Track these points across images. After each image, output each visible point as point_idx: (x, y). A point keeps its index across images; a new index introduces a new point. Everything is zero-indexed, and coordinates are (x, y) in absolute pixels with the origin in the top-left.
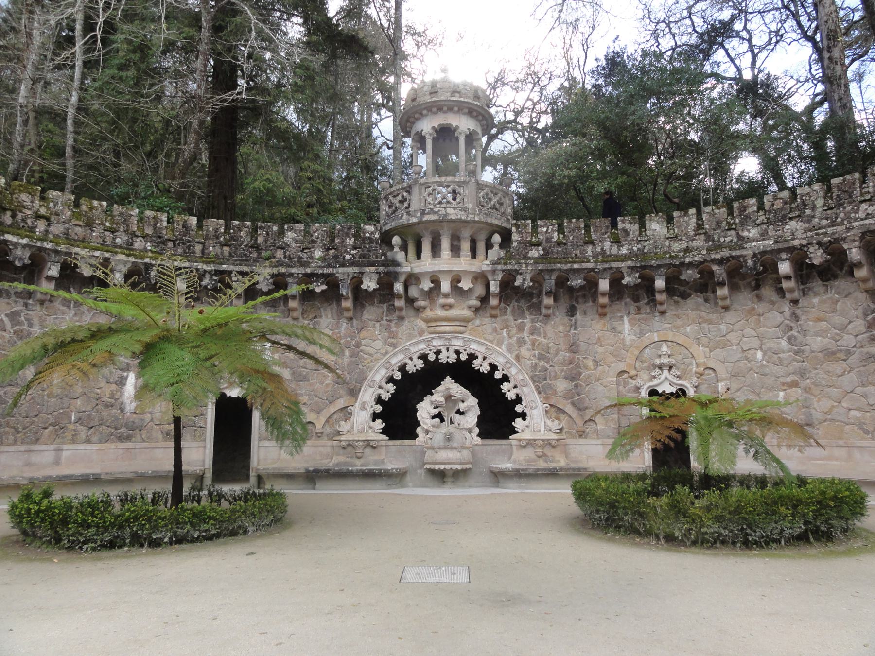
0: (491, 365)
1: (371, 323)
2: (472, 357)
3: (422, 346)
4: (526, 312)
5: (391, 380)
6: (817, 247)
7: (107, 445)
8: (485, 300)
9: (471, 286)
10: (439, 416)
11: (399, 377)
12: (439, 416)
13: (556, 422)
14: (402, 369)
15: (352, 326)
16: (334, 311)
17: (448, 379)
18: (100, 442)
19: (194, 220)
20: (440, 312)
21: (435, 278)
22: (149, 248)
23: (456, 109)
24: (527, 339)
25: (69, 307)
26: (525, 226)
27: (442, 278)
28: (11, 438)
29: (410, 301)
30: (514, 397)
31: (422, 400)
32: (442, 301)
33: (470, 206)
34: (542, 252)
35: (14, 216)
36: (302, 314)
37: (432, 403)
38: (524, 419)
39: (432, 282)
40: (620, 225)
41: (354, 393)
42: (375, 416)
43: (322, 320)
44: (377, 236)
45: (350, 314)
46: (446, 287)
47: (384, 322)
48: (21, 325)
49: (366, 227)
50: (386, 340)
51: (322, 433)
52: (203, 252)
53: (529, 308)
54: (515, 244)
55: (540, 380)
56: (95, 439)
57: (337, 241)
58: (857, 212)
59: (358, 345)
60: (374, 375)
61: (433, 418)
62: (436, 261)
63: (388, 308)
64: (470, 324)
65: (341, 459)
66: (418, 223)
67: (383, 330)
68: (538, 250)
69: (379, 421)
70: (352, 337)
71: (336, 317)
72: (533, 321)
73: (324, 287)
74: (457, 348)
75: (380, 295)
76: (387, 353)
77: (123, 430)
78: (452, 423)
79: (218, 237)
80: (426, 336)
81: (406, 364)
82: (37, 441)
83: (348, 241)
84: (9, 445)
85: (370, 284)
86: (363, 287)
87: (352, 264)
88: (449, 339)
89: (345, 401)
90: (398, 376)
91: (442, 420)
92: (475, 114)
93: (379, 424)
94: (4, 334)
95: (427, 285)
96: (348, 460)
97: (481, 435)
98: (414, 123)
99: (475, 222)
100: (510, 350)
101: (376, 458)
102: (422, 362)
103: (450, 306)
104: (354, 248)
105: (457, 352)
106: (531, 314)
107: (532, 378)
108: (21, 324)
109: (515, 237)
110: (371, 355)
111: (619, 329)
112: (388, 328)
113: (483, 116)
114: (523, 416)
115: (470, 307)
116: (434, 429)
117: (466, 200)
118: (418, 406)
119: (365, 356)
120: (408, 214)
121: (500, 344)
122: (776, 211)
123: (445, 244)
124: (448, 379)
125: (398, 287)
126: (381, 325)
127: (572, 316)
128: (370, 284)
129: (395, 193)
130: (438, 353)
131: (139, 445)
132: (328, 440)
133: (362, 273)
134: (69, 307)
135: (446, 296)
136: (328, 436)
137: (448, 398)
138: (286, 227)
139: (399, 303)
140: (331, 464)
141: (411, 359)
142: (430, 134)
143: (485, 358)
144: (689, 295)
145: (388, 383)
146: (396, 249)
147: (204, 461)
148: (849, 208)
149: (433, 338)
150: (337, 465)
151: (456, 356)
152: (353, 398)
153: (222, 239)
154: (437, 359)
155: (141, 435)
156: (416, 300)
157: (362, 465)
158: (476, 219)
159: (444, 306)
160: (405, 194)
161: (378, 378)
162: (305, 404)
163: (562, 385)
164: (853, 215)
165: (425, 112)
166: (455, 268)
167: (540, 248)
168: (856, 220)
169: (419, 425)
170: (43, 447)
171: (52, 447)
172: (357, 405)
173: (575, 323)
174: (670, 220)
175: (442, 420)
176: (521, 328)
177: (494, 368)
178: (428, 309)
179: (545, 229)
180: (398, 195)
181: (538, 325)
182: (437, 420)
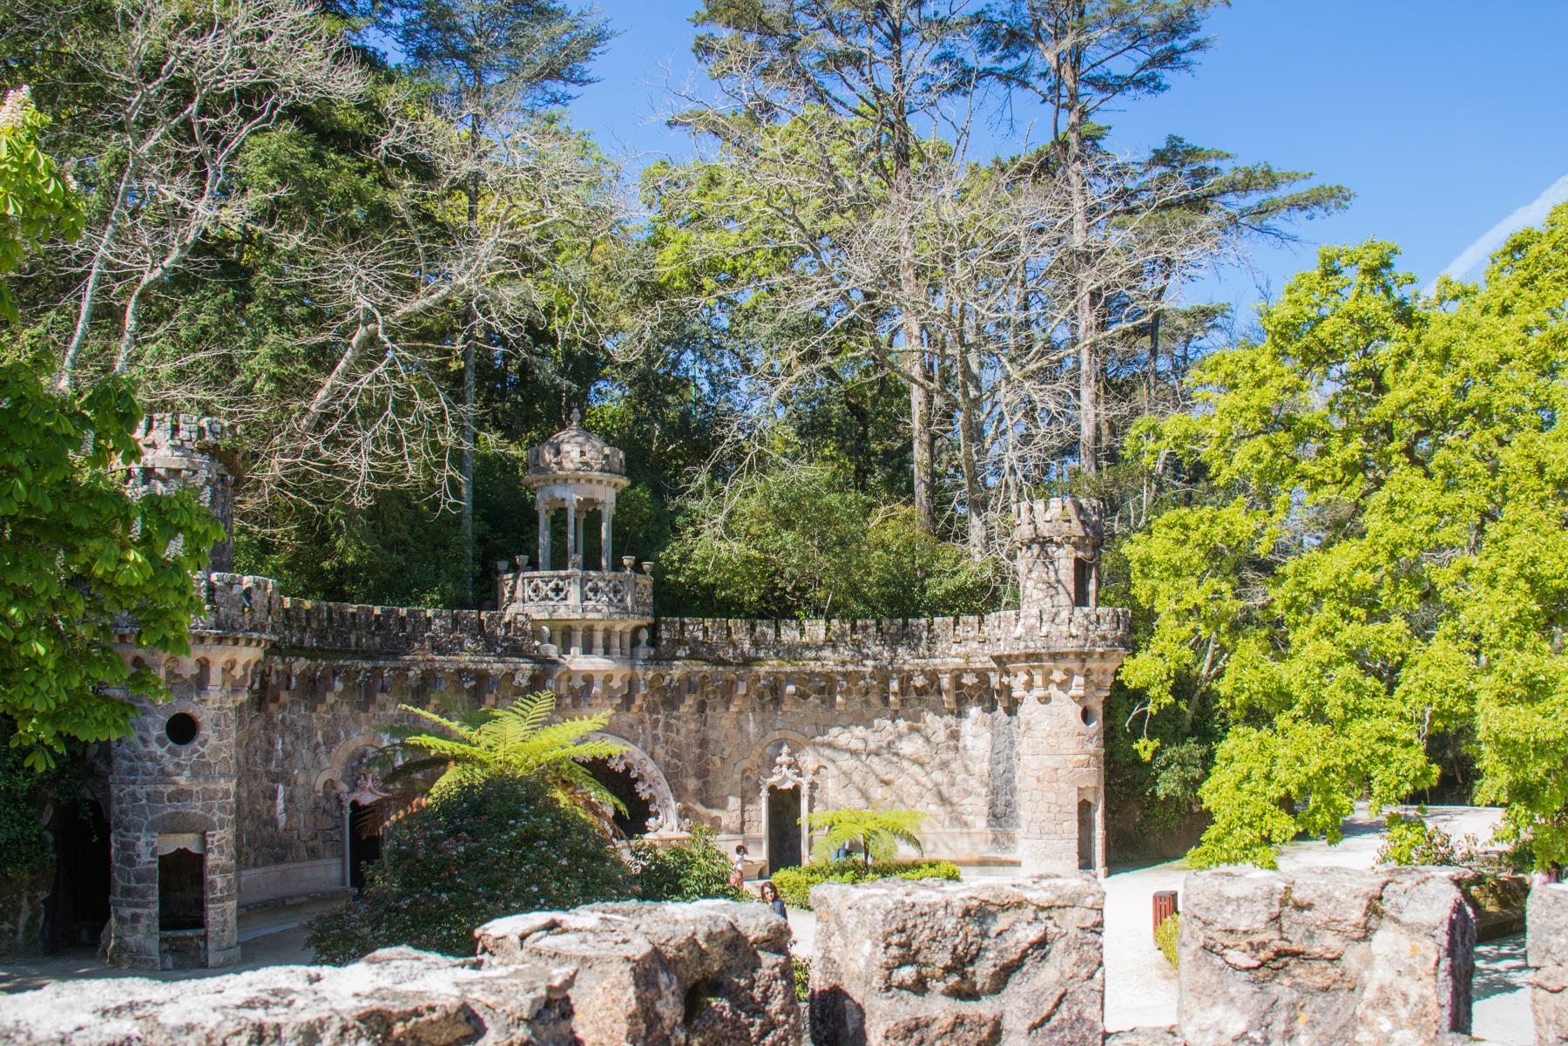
8: (628, 700)
26: (673, 623)
53: (663, 703)
55: (674, 778)
77: (277, 849)
79: (369, 626)
100: (644, 748)
109: (665, 635)
121: (635, 742)
123: (599, 639)
163: (692, 784)
176: (655, 723)
181: (672, 721)
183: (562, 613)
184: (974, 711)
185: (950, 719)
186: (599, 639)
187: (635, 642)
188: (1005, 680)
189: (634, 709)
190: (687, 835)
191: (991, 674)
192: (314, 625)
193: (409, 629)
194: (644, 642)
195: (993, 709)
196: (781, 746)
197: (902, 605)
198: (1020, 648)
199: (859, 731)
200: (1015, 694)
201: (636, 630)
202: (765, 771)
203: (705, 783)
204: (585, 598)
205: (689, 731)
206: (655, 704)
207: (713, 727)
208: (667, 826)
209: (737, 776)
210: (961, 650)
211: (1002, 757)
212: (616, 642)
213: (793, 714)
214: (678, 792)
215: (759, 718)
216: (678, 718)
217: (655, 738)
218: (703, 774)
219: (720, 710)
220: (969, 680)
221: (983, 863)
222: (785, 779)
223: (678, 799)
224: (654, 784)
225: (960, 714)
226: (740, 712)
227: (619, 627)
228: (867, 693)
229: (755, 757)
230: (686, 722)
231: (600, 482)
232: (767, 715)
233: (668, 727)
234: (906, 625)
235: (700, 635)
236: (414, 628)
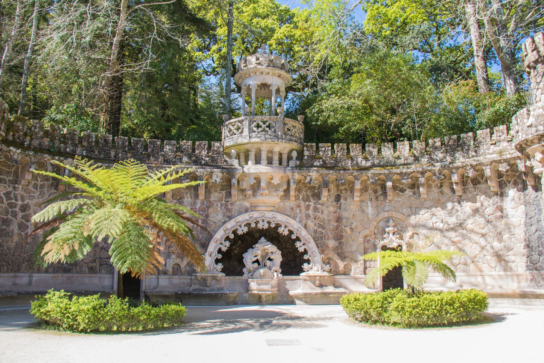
0: (289, 230)
2: (278, 226)
4: (311, 198)
5: (227, 238)
6: (470, 167)
8: (287, 191)
10: (257, 261)
13: (328, 266)
14: (234, 232)
15: (203, 204)
16: (192, 195)
22: (85, 154)
24: (311, 214)
25: (37, 189)
28: (6, 268)
30: (303, 251)
31: (247, 252)
33: (280, 133)
34: (321, 163)
36: (172, 196)
38: (309, 264)
40: (367, 149)
42: (217, 261)
50: (224, 214)
52: (115, 156)
54: (306, 157)
55: (319, 240)
57: (197, 152)
58: (489, 149)
59: (207, 216)
61: (254, 262)
62: (258, 166)
65: (197, 287)
67: (223, 208)
68: (319, 161)
69: (221, 264)
72: (315, 203)
74: (268, 220)
76: (225, 223)
78: (265, 266)
79: (124, 148)
82: (19, 271)
84: (5, 272)
90: (232, 236)
93: (220, 266)
96: (202, 287)
97: (284, 273)
100: (301, 222)
101: (218, 286)
105: (269, 223)
106: (314, 200)
107: (314, 239)
108: (12, 199)
109: (306, 153)
111: (365, 210)
114: (308, 261)
117: (277, 130)
118: (243, 255)
121: (294, 218)
122: (450, 145)
125: (234, 181)
127: (338, 201)
129: (233, 124)
130: (257, 223)
131: (75, 275)
134: (37, 189)
138: (165, 142)
140: (191, 290)
141: (240, 226)
143: (286, 227)
144: (405, 190)
147: (113, 286)
148: (485, 147)
150: (195, 290)
152: (204, 250)
153: (127, 149)
155: (76, 269)
157: (209, 291)
160: (240, 124)
163: (332, 243)
164: (487, 151)
165: (252, 74)
167: (321, 160)
168: (489, 154)
169: (245, 267)
170: (22, 274)
171: (27, 274)
172: (207, 254)
173: (340, 206)
174: (395, 147)
176: (308, 207)
177: (291, 232)
179: (323, 149)
182: (256, 264)
183: (240, 140)
184: (512, 192)
185: (496, 199)
186: (264, 156)
187: (290, 158)
188: (528, 163)
189: (292, 198)
190: (326, 274)
191: (518, 161)
192: (85, 144)
193: (149, 150)
194: (294, 158)
195: (525, 188)
196: (388, 221)
197: (460, 128)
198: (531, 134)
199: (439, 212)
200: (536, 171)
201: (291, 151)
202: (379, 236)
203: (340, 243)
204: (251, 131)
205: (329, 212)
206: (307, 195)
207: (345, 210)
208: (315, 268)
209: (361, 240)
210: (497, 149)
211: (534, 220)
212: (276, 158)
213: (396, 202)
214: (322, 248)
215: (374, 204)
216: (323, 205)
217: (308, 216)
218: (339, 237)
219: (349, 200)
220: (503, 168)
221: (524, 296)
222: (392, 241)
223: (322, 252)
224: (306, 243)
225: (502, 195)
226: (362, 201)
227: (277, 149)
228: (441, 186)
229: (372, 228)
230: (327, 207)
231: (268, 73)
232: (379, 202)
233: (316, 209)
234: (459, 138)
235: (330, 152)
236: (153, 150)
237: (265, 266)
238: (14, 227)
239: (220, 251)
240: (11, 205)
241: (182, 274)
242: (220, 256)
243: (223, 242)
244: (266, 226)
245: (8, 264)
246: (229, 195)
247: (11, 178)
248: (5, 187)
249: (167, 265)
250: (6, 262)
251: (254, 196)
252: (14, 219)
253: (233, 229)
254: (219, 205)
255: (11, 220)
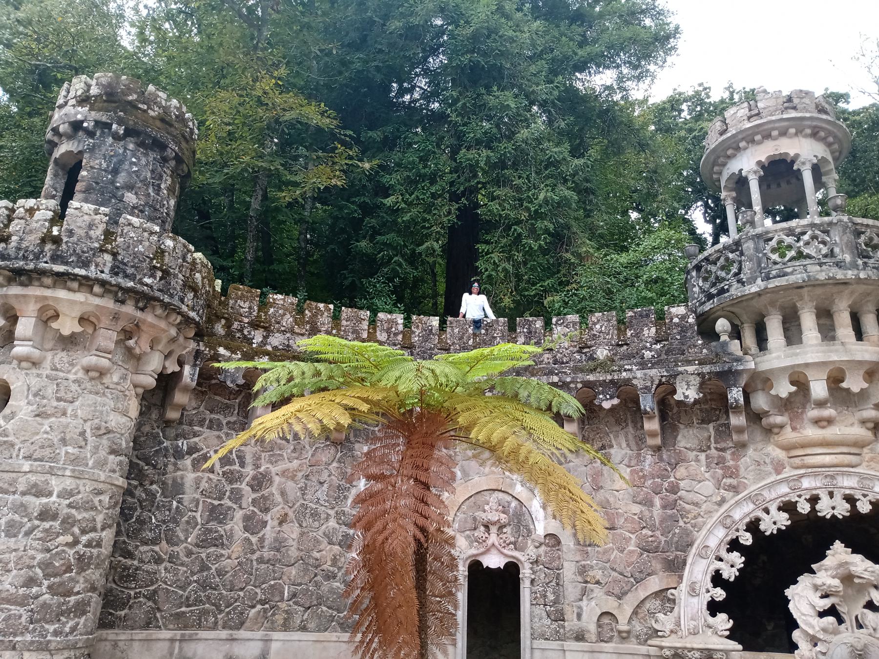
1: (692, 455)
3: (784, 489)
5: (734, 545)
7: (326, 635)
9: (865, 385)
10: (832, 611)
11: (749, 542)
12: (832, 611)
14: (753, 527)
15: (661, 459)
16: (630, 437)
17: (838, 545)
18: (319, 631)
19: (435, 321)
20: (811, 433)
21: (796, 378)
23: (792, 131)
27: (811, 375)
29: (756, 417)
32: (813, 413)
35: (228, 326)
37: (816, 588)
39: (793, 383)
41: (676, 567)
43: (612, 451)
44: (691, 320)
45: (658, 441)
46: (819, 389)
47: (713, 452)
48: (231, 465)
49: (673, 310)
50: (719, 482)
51: (628, 632)
56: (311, 625)
59: (674, 489)
60: (706, 538)
61: (822, 614)
62: (796, 349)
63: (717, 430)
64: (865, 450)
66: (759, 294)
67: (713, 465)
69: (722, 617)
70: (664, 477)
71: (634, 447)
73: (616, 401)
74: (848, 492)
75: (701, 410)
76: (723, 501)
80: (788, 473)
81: (758, 520)
82: (240, 625)
83: (646, 332)
85: (687, 392)
86: (678, 397)
87: (656, 363)
88: (832, 477)
89: (660, 581)
91: (840, 621)
92: (822, 134)
93: (723, 622)
94: (211, 476)
95: (784, 389)
98: (724, 165)
99: (859, 280)
102: (786, 515)
103: (830, 421)
104: (658, 342)
105: (850, 500)
110: (696, 504)
112: (721, 462)
113: (835, 137)
115: (863, 422)
116: (828, 637)
117: (837, 250)
118: (788, 592)
119: (687, 506)
120: (739, 281)
124: (838, 545)
125: (736, 394)
126: (707, 457)
128: (687, 392)
130: (814, 500)
132: (640, 644)
133: (675, 376)
135: (821, 404)
136: (637, 637)
137: (848, 579)
139: (737, 420)
141: (767, 511)
142: (755, 172)
145: (729, 551)
146: (724, 338)
149: (802, 476)
151: (848, 506)
154: (813, 509)
156: (766, 414)
158: (862, 275)
159: (817, 422)
161: (713, 542)
162: (598, 582)
166: (835, 358)
169: (796, 626)
171: (259, 634)
172: (684, 586)
175: (840, 621)
178: (788, 429)
180: (718, 259)
182: (831, 619)
237: (860, 626)
238: (236, 524)
239: (717, 579)
240: (231, 477)
241: (625, 636)
242: (720, 594)
243: (723, 553)
244: (842, 510)
245: (218, 607)
246: (725, 431)
247: (233, 419)
248: (219, 437)
249: (584, 616)
250: (213, 604)
251: (794, 429)
252: (235, 506)
253: (747, 520)
254: (702, 457)
255: (229, 508)
